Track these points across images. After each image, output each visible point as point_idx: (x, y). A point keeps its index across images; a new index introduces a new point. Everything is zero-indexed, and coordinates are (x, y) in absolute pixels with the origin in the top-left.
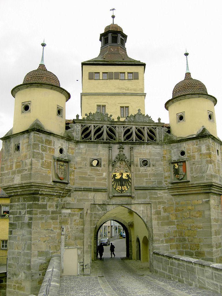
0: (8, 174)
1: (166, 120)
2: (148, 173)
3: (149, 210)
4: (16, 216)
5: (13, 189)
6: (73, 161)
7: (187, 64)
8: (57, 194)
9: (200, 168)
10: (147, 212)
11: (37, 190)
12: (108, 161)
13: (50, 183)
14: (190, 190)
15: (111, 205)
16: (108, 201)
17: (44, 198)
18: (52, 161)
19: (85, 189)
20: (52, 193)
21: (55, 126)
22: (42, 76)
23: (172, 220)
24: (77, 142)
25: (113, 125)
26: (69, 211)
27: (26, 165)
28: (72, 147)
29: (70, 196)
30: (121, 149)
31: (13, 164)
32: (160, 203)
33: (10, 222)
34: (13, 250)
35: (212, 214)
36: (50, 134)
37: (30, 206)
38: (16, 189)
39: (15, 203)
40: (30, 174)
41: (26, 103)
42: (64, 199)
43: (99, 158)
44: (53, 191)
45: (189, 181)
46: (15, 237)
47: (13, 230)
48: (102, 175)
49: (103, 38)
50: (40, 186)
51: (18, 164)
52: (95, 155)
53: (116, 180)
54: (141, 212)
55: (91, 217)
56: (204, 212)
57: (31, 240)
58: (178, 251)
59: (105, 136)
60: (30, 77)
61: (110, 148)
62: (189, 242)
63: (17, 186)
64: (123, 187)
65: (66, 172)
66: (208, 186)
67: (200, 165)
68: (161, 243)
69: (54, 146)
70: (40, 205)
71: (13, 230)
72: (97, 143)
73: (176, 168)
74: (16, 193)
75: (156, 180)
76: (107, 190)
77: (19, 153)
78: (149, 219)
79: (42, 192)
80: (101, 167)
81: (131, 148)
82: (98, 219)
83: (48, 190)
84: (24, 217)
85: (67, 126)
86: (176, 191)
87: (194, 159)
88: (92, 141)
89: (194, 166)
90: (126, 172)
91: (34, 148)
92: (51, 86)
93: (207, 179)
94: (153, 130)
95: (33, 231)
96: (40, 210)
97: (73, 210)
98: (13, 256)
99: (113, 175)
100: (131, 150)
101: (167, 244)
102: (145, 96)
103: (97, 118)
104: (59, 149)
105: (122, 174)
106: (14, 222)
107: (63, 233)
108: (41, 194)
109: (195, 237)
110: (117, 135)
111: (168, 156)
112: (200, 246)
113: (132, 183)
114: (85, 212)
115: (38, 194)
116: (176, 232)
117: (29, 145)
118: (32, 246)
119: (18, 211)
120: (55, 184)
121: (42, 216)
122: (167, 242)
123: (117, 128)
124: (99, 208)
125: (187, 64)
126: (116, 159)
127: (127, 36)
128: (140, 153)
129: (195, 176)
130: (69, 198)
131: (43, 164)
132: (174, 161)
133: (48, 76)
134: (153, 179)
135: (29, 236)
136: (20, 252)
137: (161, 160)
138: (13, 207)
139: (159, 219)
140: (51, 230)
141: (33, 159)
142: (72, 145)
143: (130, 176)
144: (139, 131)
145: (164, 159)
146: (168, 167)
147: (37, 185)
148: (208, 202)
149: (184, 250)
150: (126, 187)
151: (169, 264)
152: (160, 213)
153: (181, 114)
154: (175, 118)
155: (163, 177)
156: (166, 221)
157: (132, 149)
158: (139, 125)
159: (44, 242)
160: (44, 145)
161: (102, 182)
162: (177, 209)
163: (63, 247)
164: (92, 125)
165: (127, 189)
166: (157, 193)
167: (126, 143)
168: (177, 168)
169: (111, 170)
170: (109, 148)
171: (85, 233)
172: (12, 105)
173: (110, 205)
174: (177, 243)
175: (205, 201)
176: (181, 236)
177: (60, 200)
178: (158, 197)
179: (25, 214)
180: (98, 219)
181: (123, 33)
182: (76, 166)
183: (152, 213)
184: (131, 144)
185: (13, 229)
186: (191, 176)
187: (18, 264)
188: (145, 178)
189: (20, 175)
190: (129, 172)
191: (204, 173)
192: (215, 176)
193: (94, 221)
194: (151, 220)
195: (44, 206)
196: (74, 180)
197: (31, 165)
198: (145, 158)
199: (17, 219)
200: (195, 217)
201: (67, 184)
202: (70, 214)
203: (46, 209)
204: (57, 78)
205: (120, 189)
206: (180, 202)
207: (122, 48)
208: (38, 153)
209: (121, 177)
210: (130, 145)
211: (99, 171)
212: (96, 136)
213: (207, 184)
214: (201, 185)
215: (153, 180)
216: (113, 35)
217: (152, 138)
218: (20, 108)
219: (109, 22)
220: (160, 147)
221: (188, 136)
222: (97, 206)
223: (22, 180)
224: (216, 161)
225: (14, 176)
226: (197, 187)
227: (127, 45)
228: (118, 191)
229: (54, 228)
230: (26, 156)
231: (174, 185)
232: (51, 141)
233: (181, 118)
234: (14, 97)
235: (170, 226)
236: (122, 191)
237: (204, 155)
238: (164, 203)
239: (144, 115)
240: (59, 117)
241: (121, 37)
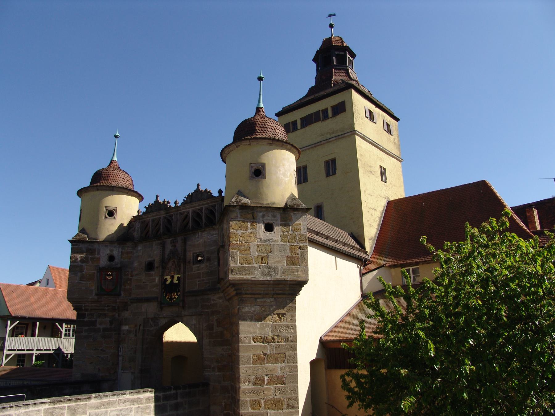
105: (172, 277)
165: (177, 297)
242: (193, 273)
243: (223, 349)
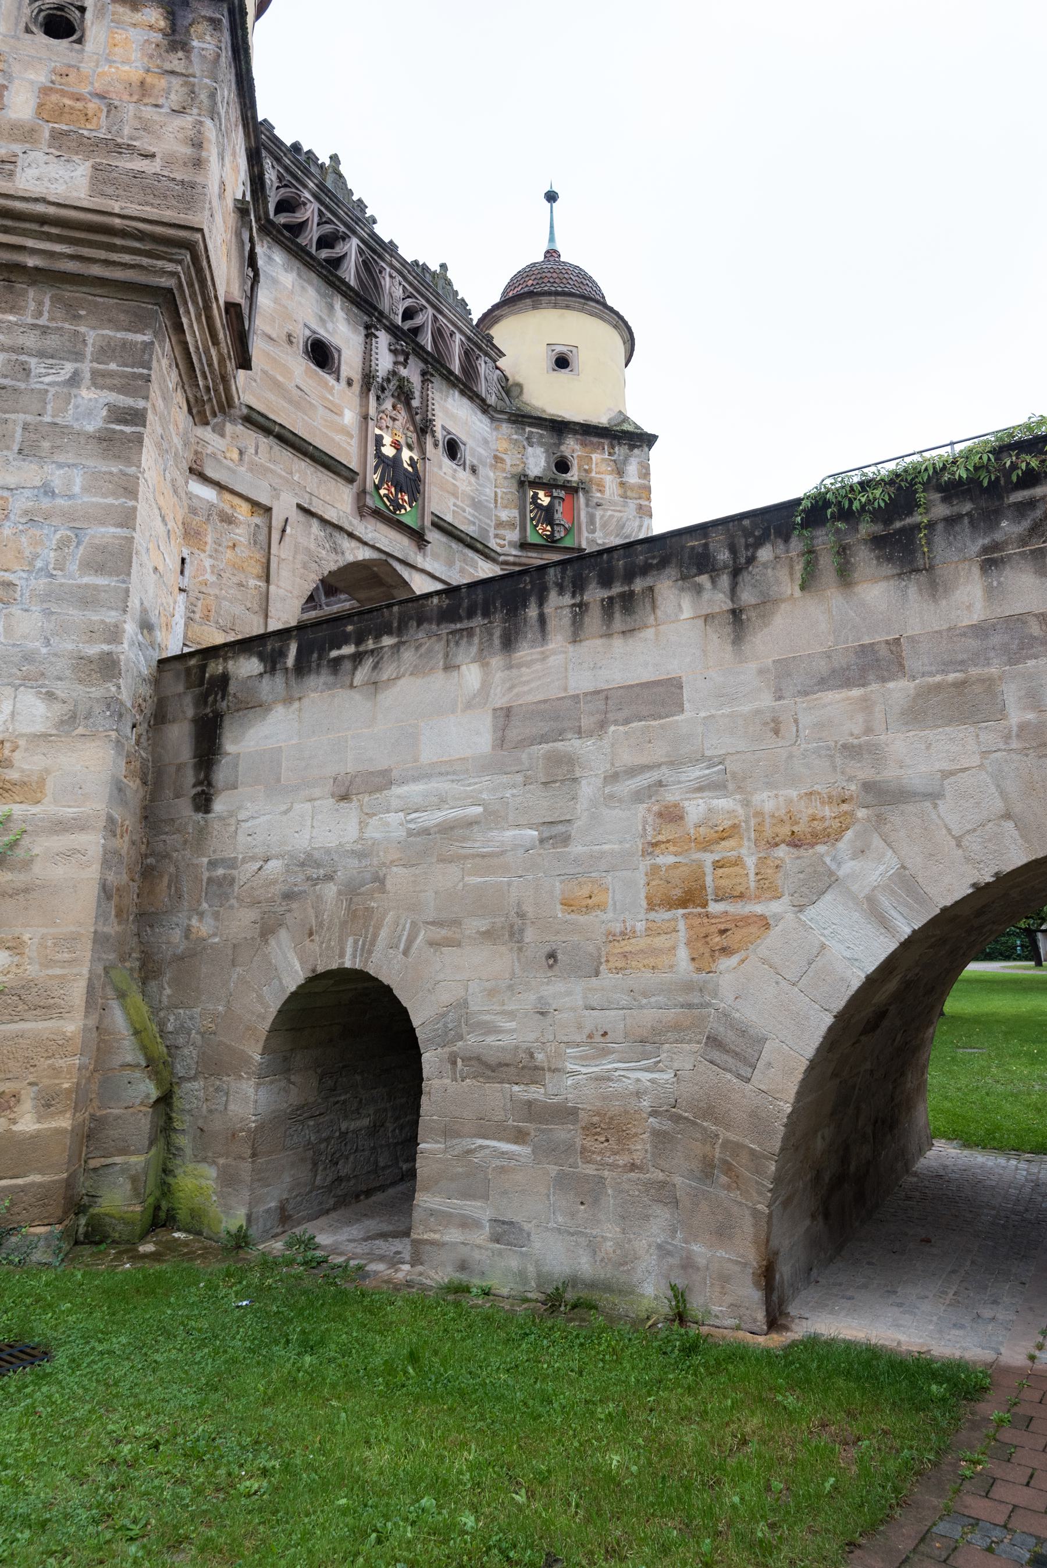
7: (552, 227)
67: (616, 514)
89: (598, 513)
111: (510, 460)
125: (552, 227)
134: (469, 513)
153: (564, 349)
168: (545, 503)
211: (331, 390)
220: (485, 419)
231: (530, 554)
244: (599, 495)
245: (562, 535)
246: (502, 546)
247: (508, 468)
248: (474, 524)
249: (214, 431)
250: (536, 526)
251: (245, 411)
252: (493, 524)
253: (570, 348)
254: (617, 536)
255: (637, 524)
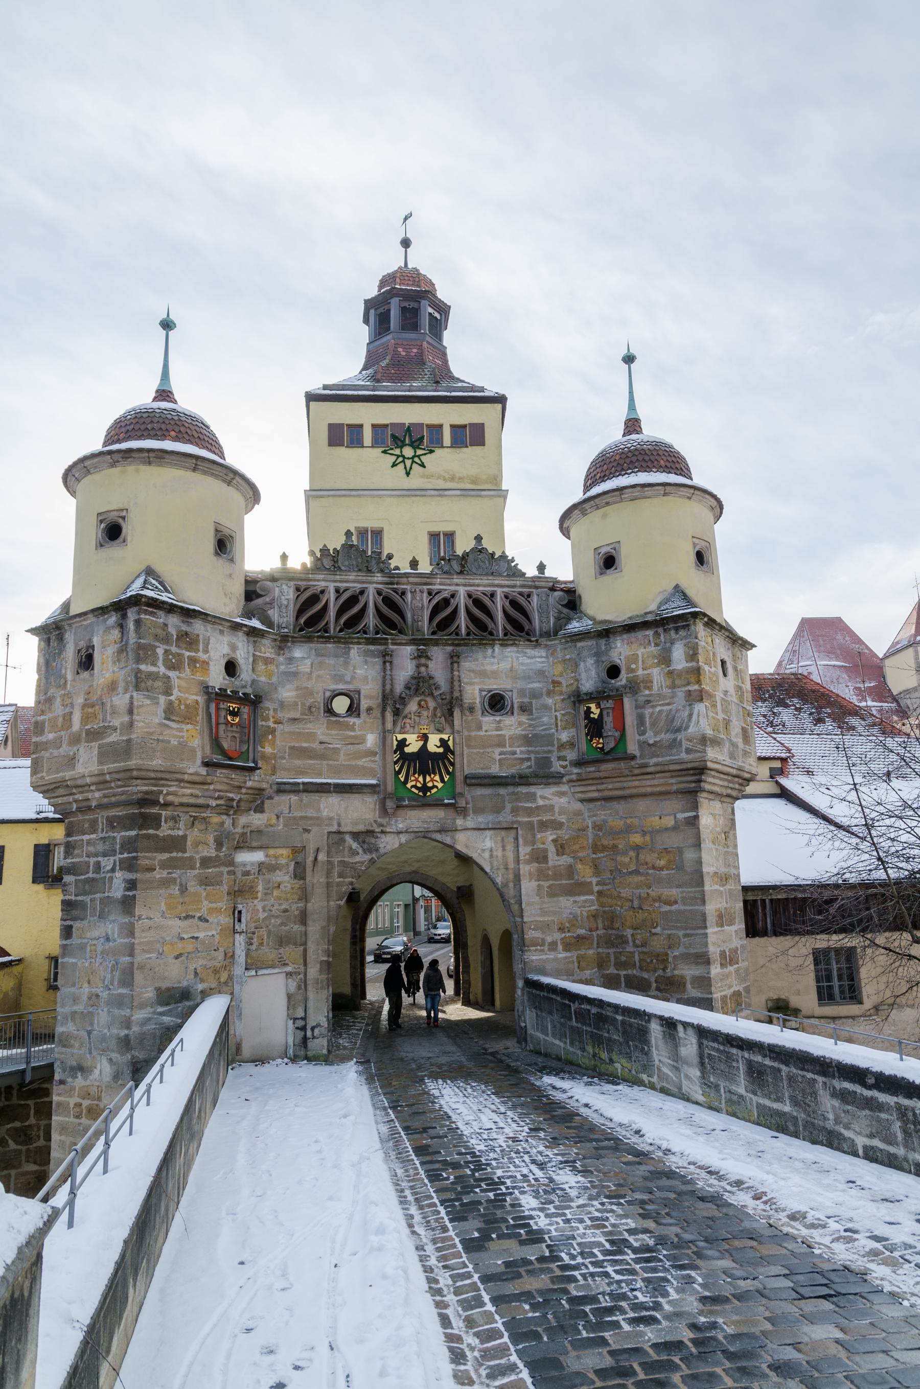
0: (57, 744)
1: (562, 569)
2: (507, 733)
3: (510, 847)
4: (83, 877)
5: (74, 791)
6: (271, 700)
7: (631, 393)
8: (219, 802)
9: (667, 716)
10: (504, 856)
11: (152, 792)
12: (381, 696)
13: (194, 768)
14: (637, 783)
15: (393, 836)
16: (384, 821)
17: (175, 819)
18: (201, 699)
19: (310, 788)
20: (201, 801)
21: (209, 589)
22: (163, 426)
23: (583, 880)
24: (283, 642)
25: (395, 586)
26: (258, 856)
27: (113, 713)
28: (268, 655)
29: (260, 809)
30: (423, 661)
31: (71, 713)
32: (544, 825)
33: (67, 897)
34: (72, 990)
35: (706, 857)
36: (188, 614)
37: (129, 845)
38: (82, 793)
39: (80, 838)
40: (129, 741)
41: (113, 516)
42: (243, 820)
43: (351, 687)
44: (207, 794)
45: (633, 758)
46: (82, 947)
47: (77, 925)
48: (363, 740)
49: (372, 312)
50: (162, 779)
51: (90, 710)
52: (339, 678)
53: (405, 758)
54: (487, 855)
55: (328, 874)
56: (680, 851)
57: (131, 955)
58: (603, 976)
59: (371, 619)
60: (123, 430)
61: (387, 658)
62: (637, 946)
63: (88, 780)
64: (428, 778)
65: (251, 734)
66: (692, 772)
68: (549, 950)
69: (206, 651)
70: (164, 839)
71: (77, 925)
72: (347, 642)
73: (592, 715)
74: (84, 804)
75: (533, 756)
76: (377, 789)
77: (92, 675)
78: (511, 876)
79: (170, 798)
80: (359, 715)
81: (452, 657)
82: (350, 879)
83: (188, 791)
84: (111, 879)
85: (251, 588)
86: (594, 788)
87: (649, 688)
88: (329, 637)
89: (647, 712)
90: (440, 731)
91: (138, 660)
92: (194, 461)
93: (688, 751)
94: (522, 601)
95: (138, 925)
96: (165, 856)
97: (271, 852)
98: (75, 1008)
99: (395, 743)
100: (452, 663)
101: (568, 954)
102: (505, 497)
103: (347, 563)
104: (223, 663)
105: (425, 738)
106: (80, 898)
107: (243, 926)
108: (167, 805)
109: (653, 931)
110: (409, 616)
112: (670, 959)
113: (458, 766)
114: (310, 860)
115: (155, 803)
116: (594, 916)
117: (123, 649)
118: (135, 971)
119: (92, 860)
120: (210, 769)
121: (169, 873)
122: (567, 947)
123: (409, 596)
124: (355, 845)
125: (631, 393)
126: (407, 692)
127: (450, 307)
128: (483, 674)
129: (651, 742)
130: (258, 815)
131: (170, 712)
132: (586, 694)
133: (182, 429)
134: (522, 752)
135: (127, 940)
136: (97, 996)
137: (549, 693)
138: (74, 848)
139: (541, 875)
140: (200, 918)
141: (135, 694)
142: (267, 648)
143: (450, 743)
144: (478, 603)
145: (557, 689)
146: (569, 713)
147: (152, 775)
148: (693, 822)
149: (622, 973)
150: (437, 778)
151: (570, 1019)
152: (545, 859)
153: (608, 549)
154: (591, 562)
155: (553, 745)
156: (564, 882)
157: (455, 659)
158: (478, 585)
159: (177, 958)
160: (174, 649)
161: (361, 763)
162: (599, 843)
163: (239, 970)
164: (331, 587)
165: (440, 785)
166: (535, 794)
167: (436, 643)
168: (596, 716)
169: (389, 725)
170: (384, 656)
171: (310, 922)
172: (60, 519)
173: (388, 835)
174: (600, 950)
175: (685, 818)
176: (612, 929)
177: (228, 822)
178: (538, 808)
179: (113, 870)
180: (350, 879)
181: (435, 296)
182: (280, 715)
183: (522, 858)
184: (453, 645)
185: (74, 919)
186: (639, 741)
187: (89, 1033)
188: (498, 751)
189: (95, 744)
190: (448, 729)
191: (678, 730)
192: (716, 742)
193: (339, 884)
194: (517, 878)
195: (177, 844)
196: (275, 758)
197: (131, 712)
198: (495, 685)
199: (87, 887)
200: (654, 868)
201: (251, 770)
202: (261, 864)
203: (185, 851)
204: (214, 435)
205: (419, 785)
206: (605, 821)
207: (434, 346)
208: (154, 676)
209: (424, 748)
210: (449, 648)
211: (352, 728)
212: (342, 621)
213: (689, 766)
214: (672, 767)
215: (521, 756)
216: (406, 304)
217: (518, 627)
218: (94, 532)
219: (392, 261)
221: (630, 618)
222: (348, 838)
223: (100, 763)
224: (719, 695)
225: (75, 748)
226: (658, 775)
227: (448, 337)
228: (413, 790)
229: (211, 911)
230: (112, 687)
231: (588, 769)
232: (198, 635)
233: (609, 562)
234: (73, 493)
235: (578, 898)
236: (425, 789)
237: (680, 674)
238: (557, 825)
239: (493, 554)
240: (220, 563)
241: (430, 310)
242: (482, 733)
243: (575, 902)
244: (647, 692)
245: (612, 745)
246: (564, 767)
247: (564, 689)
248: (529, 759)
249: (255, 812)
250: (591, 740)
251: (275, 787)
252: (555, 748)
253: (612, 546)
254: (668, 731)
255: (687, 713)
